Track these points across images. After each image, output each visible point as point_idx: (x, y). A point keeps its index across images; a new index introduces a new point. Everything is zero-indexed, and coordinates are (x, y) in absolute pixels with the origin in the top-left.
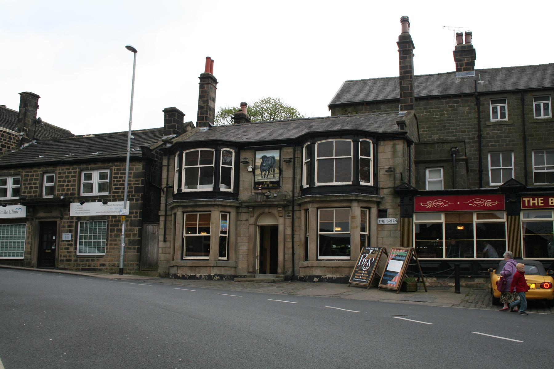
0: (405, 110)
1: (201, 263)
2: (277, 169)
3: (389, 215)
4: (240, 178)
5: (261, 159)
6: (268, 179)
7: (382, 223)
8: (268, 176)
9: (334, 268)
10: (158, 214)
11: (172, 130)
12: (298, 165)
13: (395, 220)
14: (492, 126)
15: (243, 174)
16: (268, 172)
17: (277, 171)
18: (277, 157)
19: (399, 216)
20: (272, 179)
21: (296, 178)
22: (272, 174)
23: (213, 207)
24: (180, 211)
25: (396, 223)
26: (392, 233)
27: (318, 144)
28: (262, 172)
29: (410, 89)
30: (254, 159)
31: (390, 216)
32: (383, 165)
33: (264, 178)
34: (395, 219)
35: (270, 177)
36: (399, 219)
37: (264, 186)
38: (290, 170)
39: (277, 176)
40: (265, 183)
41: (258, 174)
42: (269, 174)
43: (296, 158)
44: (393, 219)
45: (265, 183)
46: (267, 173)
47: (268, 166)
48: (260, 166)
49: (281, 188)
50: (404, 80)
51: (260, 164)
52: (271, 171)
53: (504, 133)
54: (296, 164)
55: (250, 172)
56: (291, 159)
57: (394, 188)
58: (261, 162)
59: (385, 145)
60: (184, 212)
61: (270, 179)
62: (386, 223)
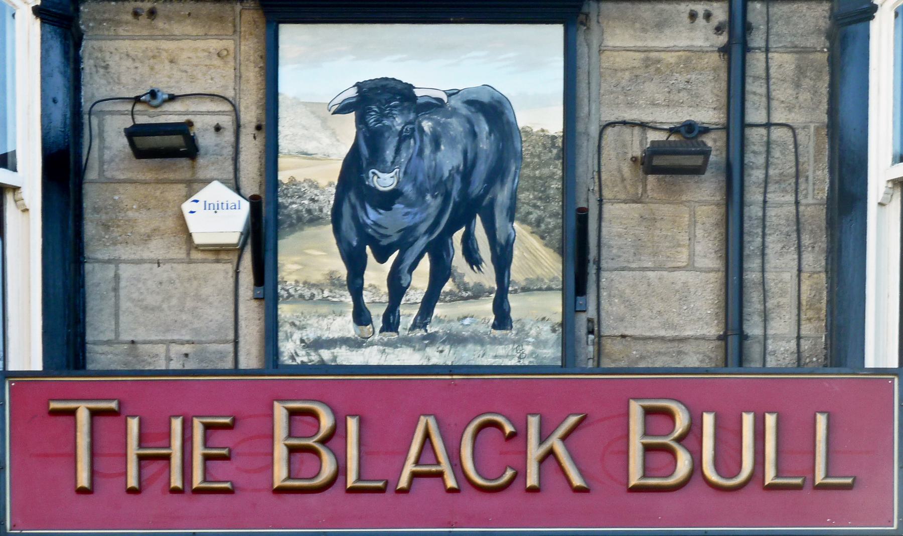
4: (91, 318)
5: (351, 117)
6: (432, 339)
12: (771, 212)
16: (425, 264)
20: (478, 339)
22: (477, 293)
30: (250, 115)
33: (390, 323)
35: (456, 326)
41: (317, 277)
42: (448, 286)
47: (433, 203)
48: (328, 199)
51: (338, 166)
52: (473, 258)
55: (217, 251)
56: (690, 129)
58: (345, 148)
61: (455, 340)
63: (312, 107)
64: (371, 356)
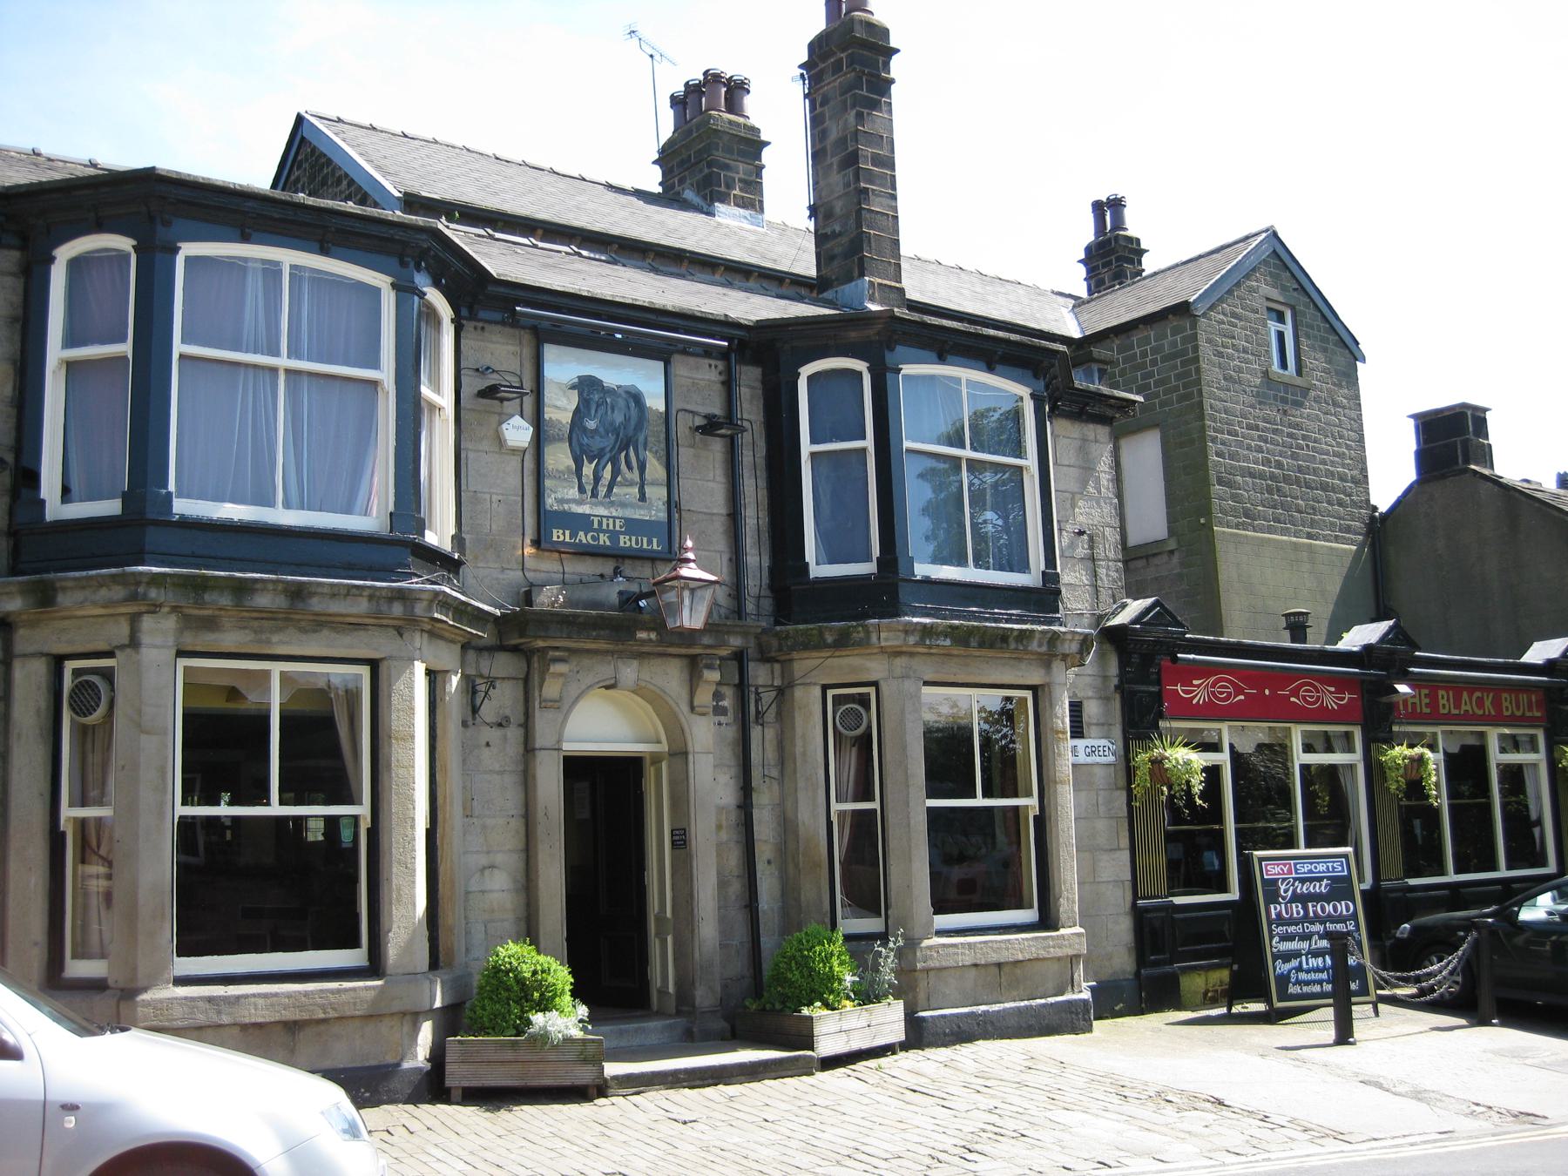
2: (655, 462)
3: (1089, 724)
6: (612, 504)
16: (609, 467)
17: (655, 469)
18: (655, 401)
19: (1117, 731)
20: (632, 506)
22: (631, 484)
24: (158, 641)
25: (1111, 759)
33: (594, 494)
36: (1120, 743)
37: (593, 537)
38: (711, 475)
39: (657, 494)
40: (600, 523)
41: (562, 468)
42: (619, 479)
45: (600, 523)
46: (607, 473)
47: (612, 438)
55: (514, 451)
61: (623, 505)
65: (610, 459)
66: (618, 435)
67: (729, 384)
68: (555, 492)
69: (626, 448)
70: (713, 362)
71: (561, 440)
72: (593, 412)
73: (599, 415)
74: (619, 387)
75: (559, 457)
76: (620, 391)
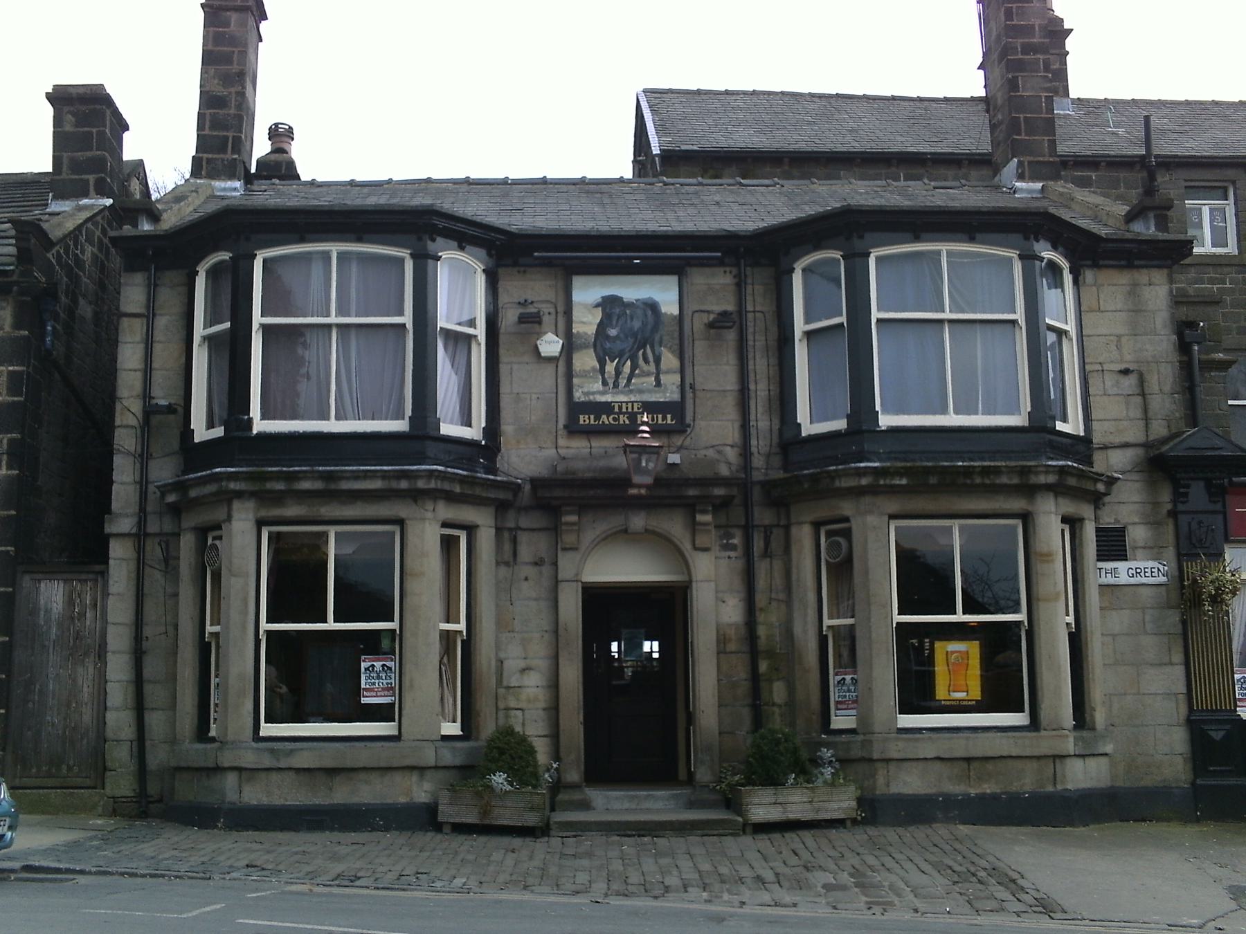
0: (1034, 178)
1: (363, 756)
2: (670, 356)
3: (1135, 548)
4: (501, 384)
5: (600, 309)
6: (631, 391)
7: (1110, 580)
8: (629, 380)
9: (975, 765)
10: (103, 528)
11: (91, 178)
12: (757, 343)
13: (1159, 570)
14: (1193, 270)
15: (515, 367)
16: (629, 363)
19: (1170, 553)
20: (649, 391)
21: (752, 394)
22: (648, 374)
23: (416, 501)
25: (1163, 579)
26: (1148, 618)
27: (878, 259)
28: (602, 364)
29: (1047, 108)
30: (561, 309)
31: (1139, 553)
32: (1101, 359)
33: (616, 385)
34: (1155, 564)
35: (640, 386)
36: (1174, 565)
37: (614, 419)
39: (671, 381)
40: (620, 408)
41: (588, 368)
42: (637, 372)
43: (750, 316)
44: (1151, 564)
45: (620, 408)
47: (631, 340)
49: (689, 430)
50: (1025, 74)
52: (646, 361)
53: (1232, 291)
54: (750, 337)
57: (1146, 445)
59: (1098, 286)
60: (260, 523)
61: (641, 391)
62: (1123, 579)
63: (585, 306)
64: (608, 398)
65: (629, 357)
66: (636, 338)
67: (740, 285)
68: (582, 387)
69: (644, 347)
70: (728, 269)
71: (586, 347)
72: (614, 322)
73: (620, 323)
74: (637, 300)
75: (585, 360)
76: (638, 303)
